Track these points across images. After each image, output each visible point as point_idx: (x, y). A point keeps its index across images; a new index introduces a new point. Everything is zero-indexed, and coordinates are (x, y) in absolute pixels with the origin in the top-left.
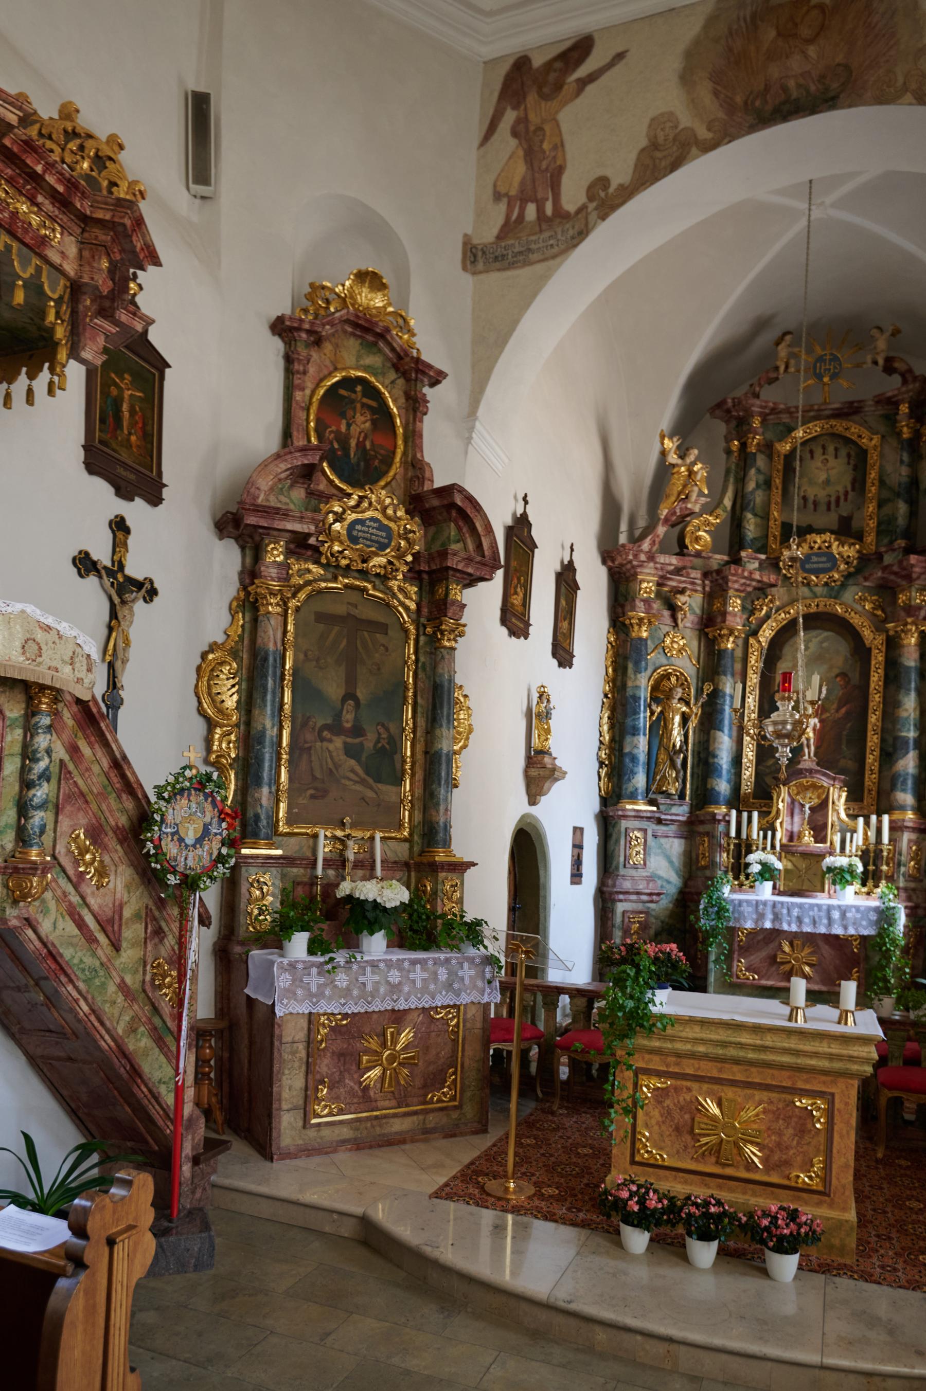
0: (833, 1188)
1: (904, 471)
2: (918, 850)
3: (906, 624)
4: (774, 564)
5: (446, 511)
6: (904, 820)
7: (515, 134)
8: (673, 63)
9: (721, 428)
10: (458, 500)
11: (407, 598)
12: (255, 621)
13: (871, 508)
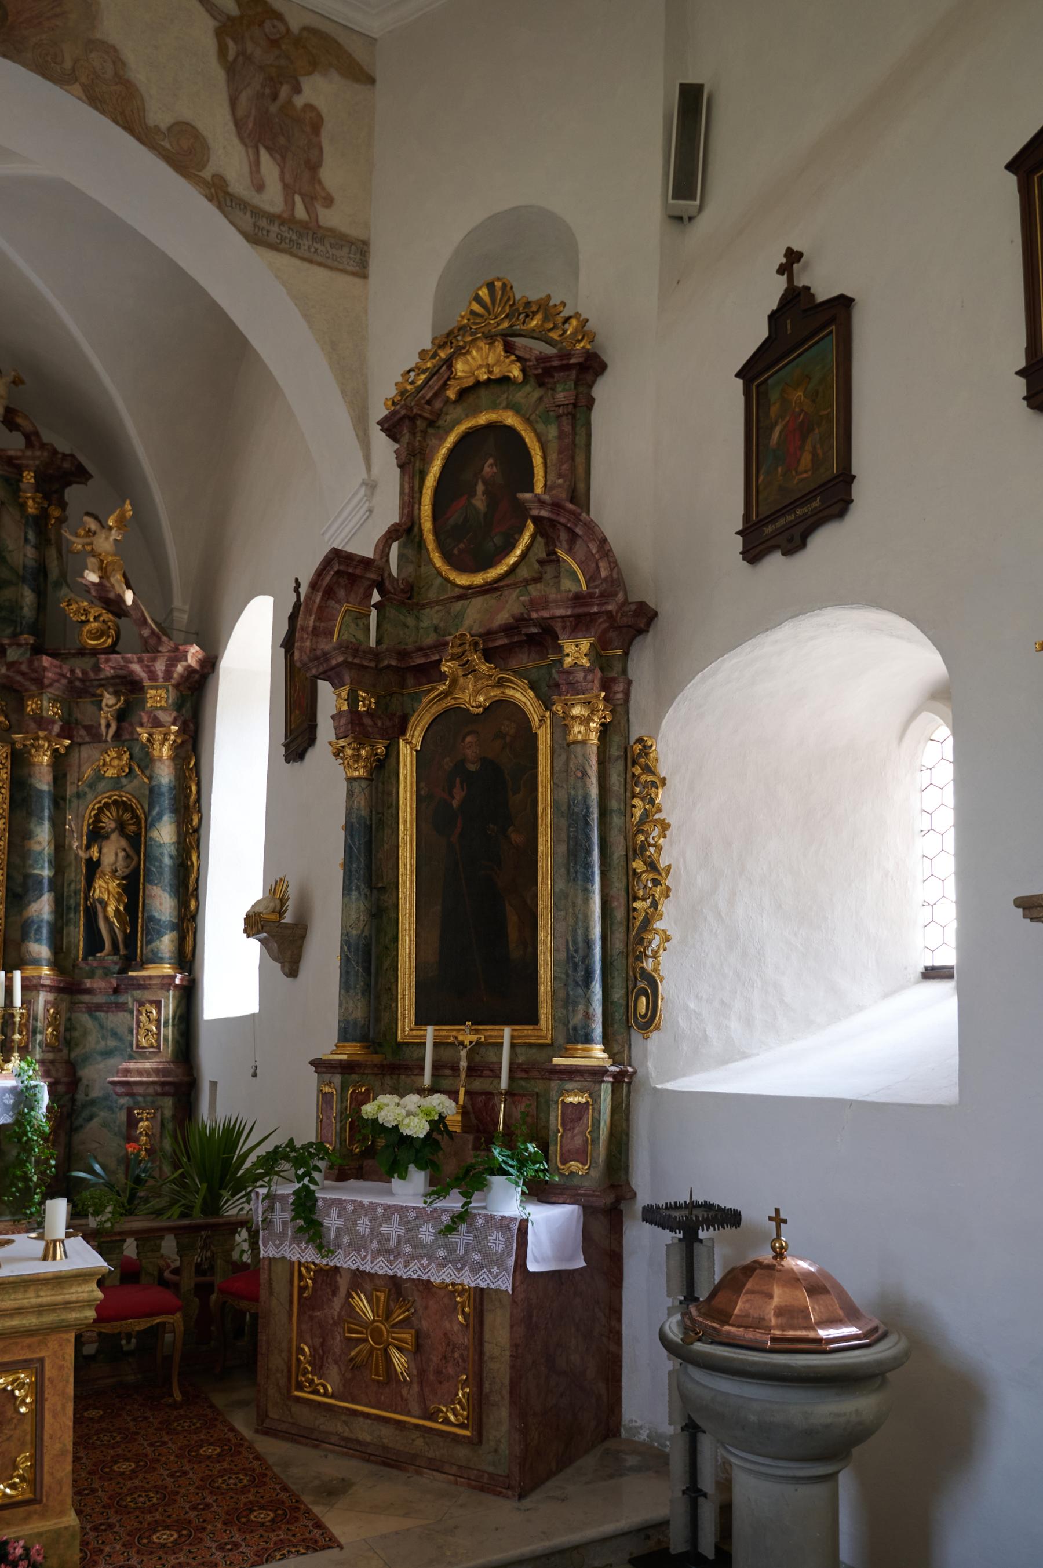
0: (45, 1489)
2: (56, 1013)
3: (37, 739)
6: (40, 977)
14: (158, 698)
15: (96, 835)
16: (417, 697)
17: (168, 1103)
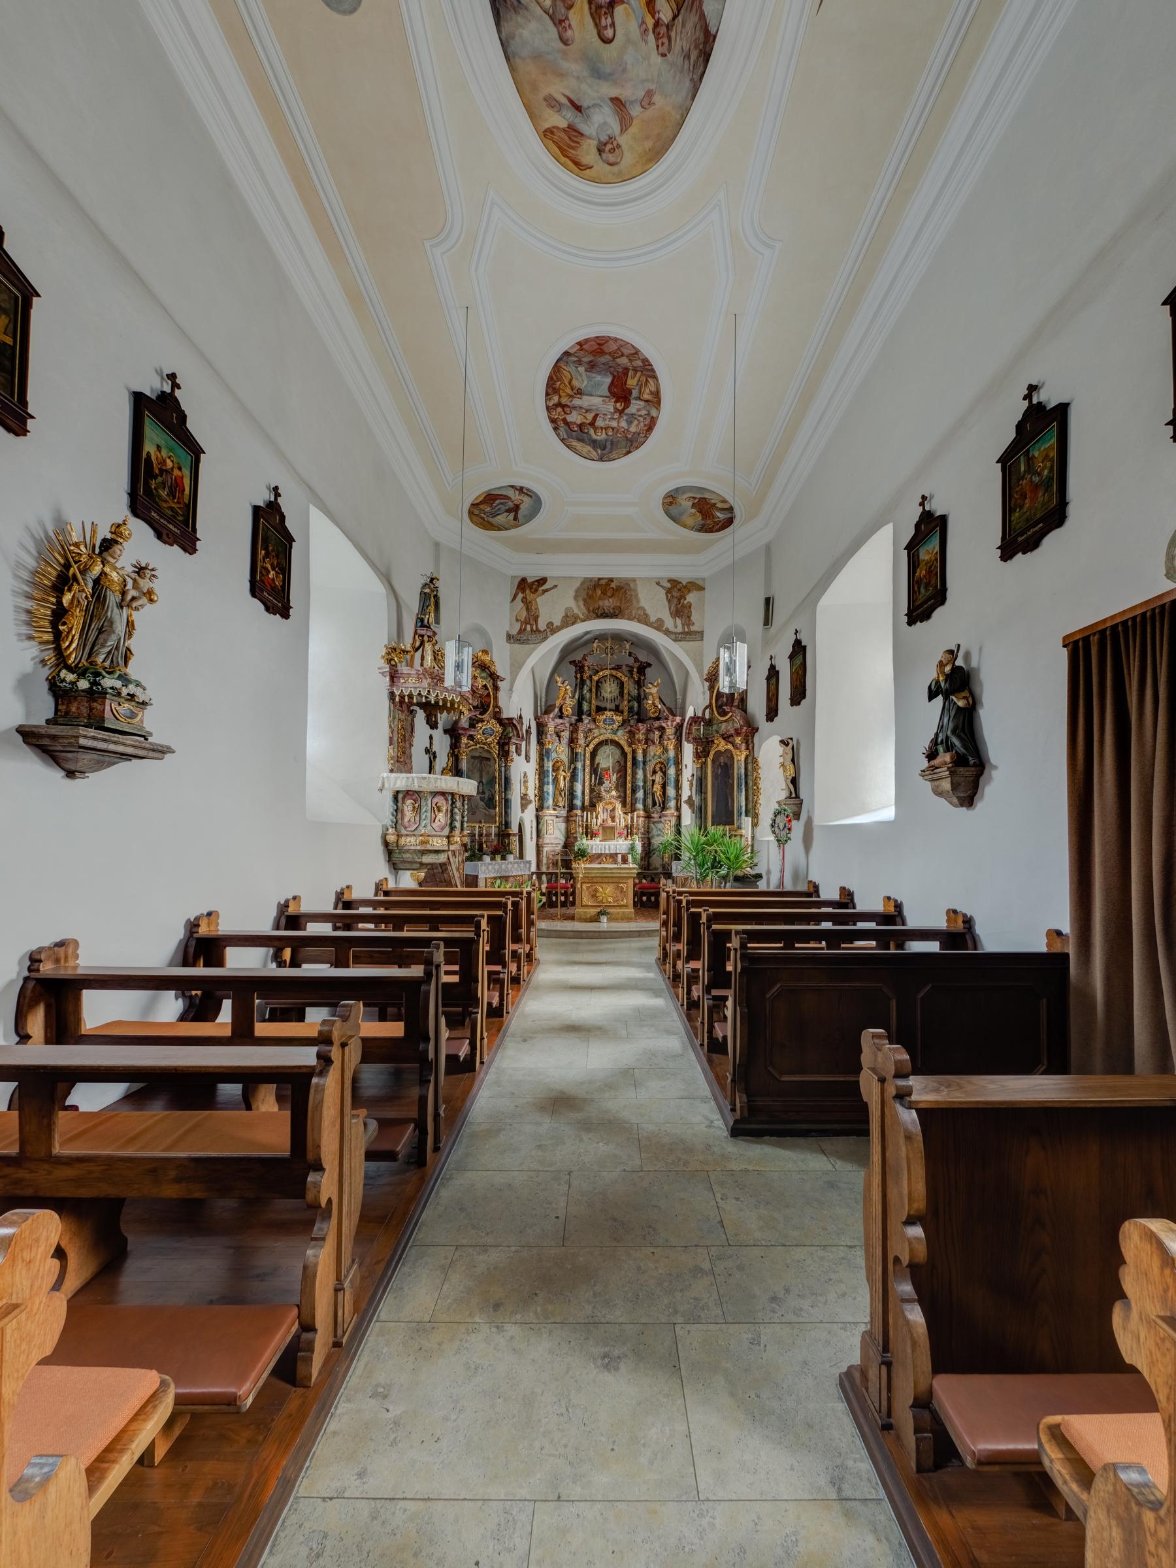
4: (594, 721)
8: (572, 593)
9: (573, 669)
11: (495, 750)
14: (670, 732)
15: (654, 772)
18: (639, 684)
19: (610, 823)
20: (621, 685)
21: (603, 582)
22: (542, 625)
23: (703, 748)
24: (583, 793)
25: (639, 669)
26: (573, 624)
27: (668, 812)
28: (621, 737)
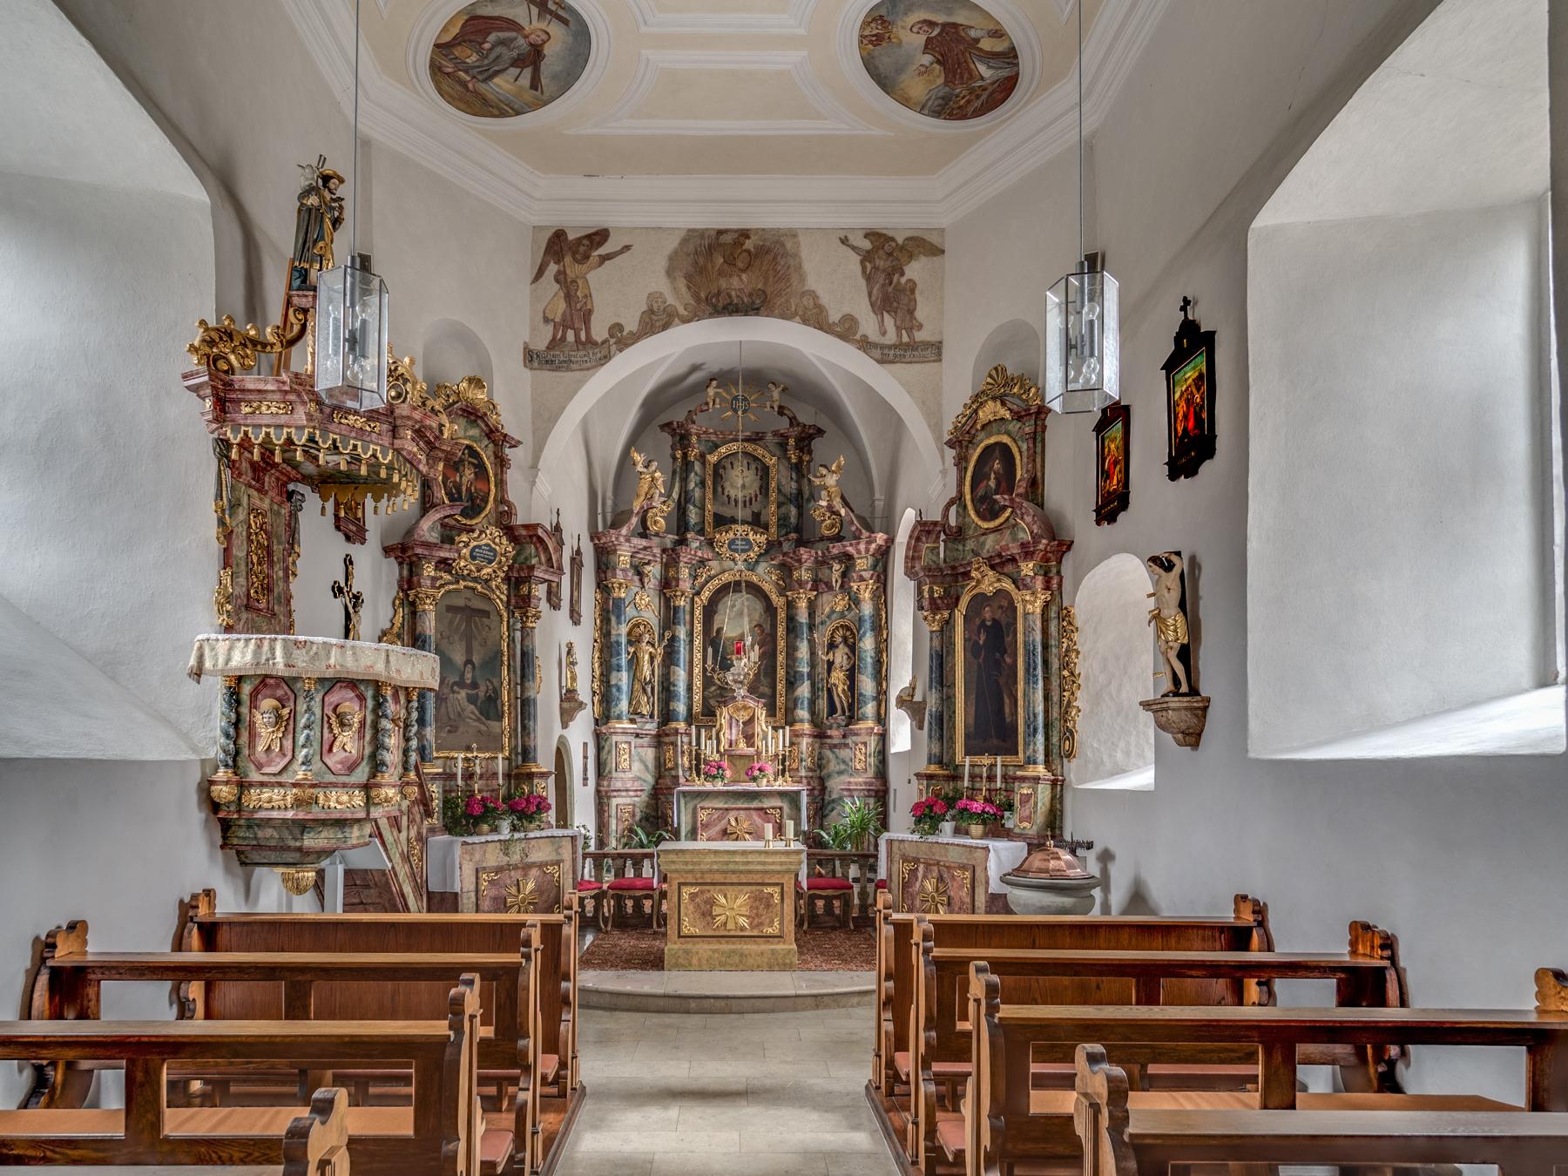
1: (794, 485)
4: (710, 543)
5: (526, 538)
7: (557, 281)
8: (661, 263)
9: (667, 439)
10: (540, 532)
11: (500, 596)
12: (414, 613)
13: (773, 508)
14: (863, 564)
15: (832, 646)
16: (963, 587)
17: (871, 801)
18: (799, 470)
19: (742, 747)
20: (764, 472)
21: (727, 239)
22: (599, 332)
23: (943, 586)
24: (690, 688)
25: (799, 440)
26: (665, 327)
27: (861, 725)
28: (766, 576)
